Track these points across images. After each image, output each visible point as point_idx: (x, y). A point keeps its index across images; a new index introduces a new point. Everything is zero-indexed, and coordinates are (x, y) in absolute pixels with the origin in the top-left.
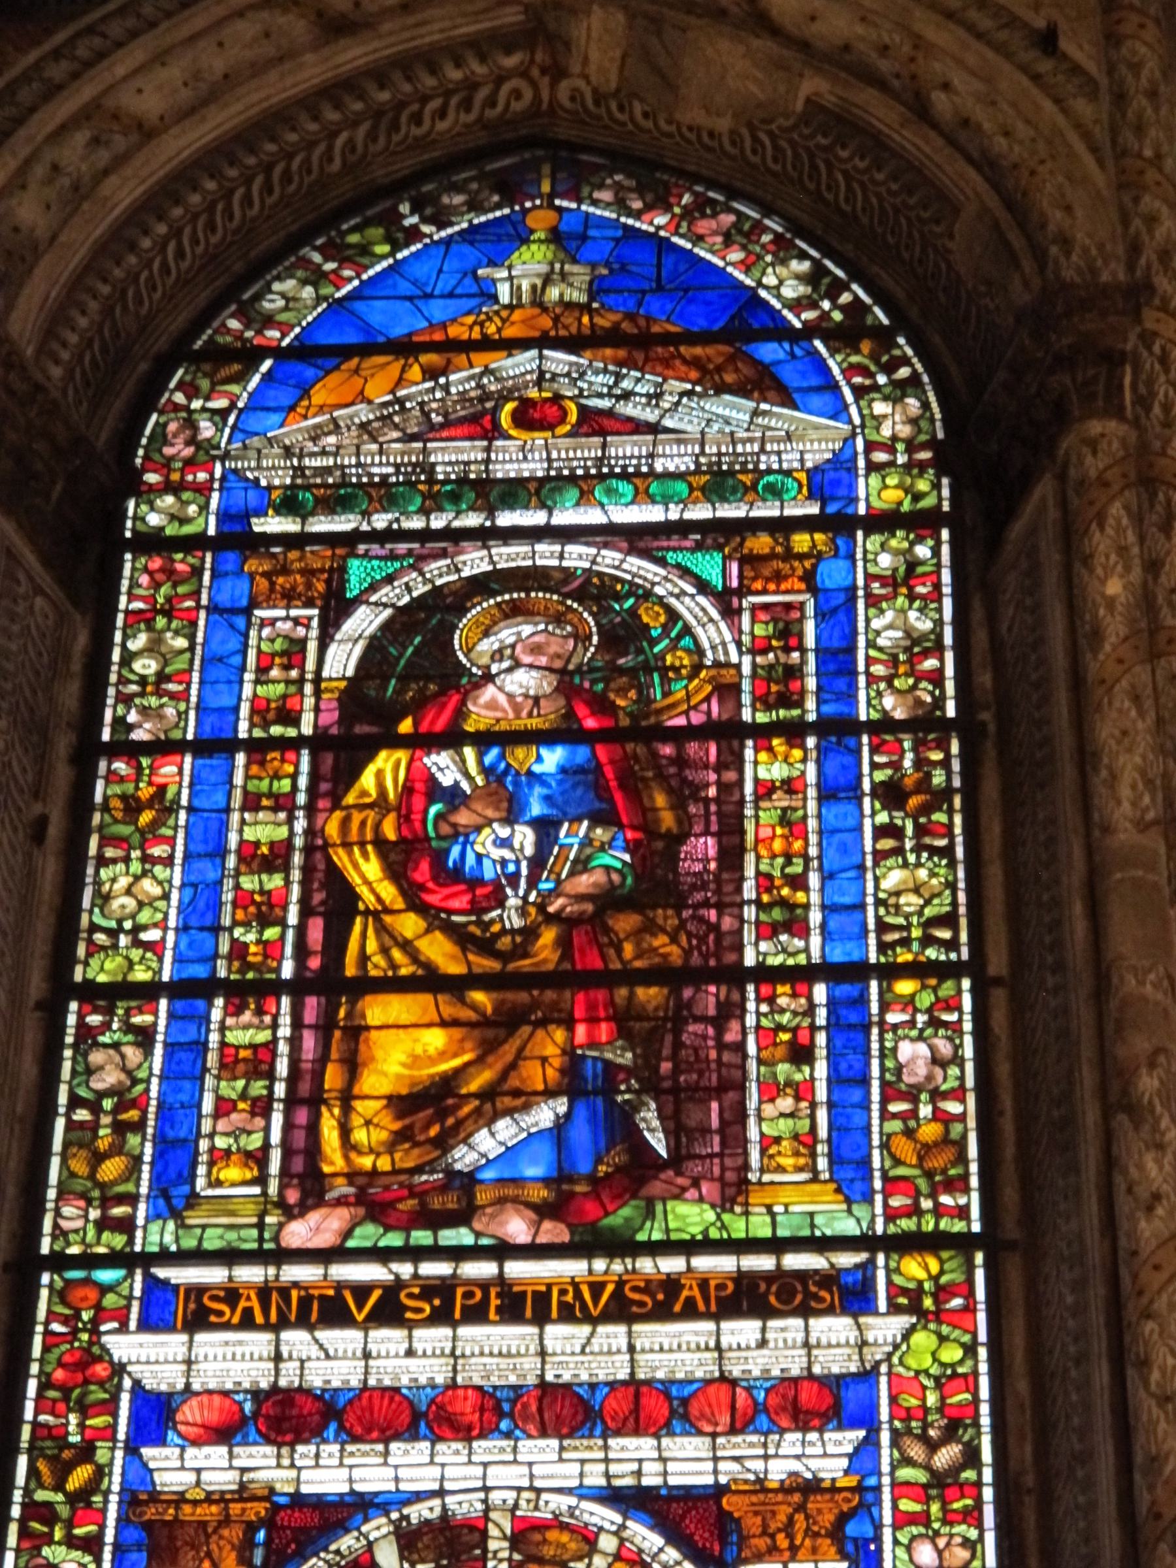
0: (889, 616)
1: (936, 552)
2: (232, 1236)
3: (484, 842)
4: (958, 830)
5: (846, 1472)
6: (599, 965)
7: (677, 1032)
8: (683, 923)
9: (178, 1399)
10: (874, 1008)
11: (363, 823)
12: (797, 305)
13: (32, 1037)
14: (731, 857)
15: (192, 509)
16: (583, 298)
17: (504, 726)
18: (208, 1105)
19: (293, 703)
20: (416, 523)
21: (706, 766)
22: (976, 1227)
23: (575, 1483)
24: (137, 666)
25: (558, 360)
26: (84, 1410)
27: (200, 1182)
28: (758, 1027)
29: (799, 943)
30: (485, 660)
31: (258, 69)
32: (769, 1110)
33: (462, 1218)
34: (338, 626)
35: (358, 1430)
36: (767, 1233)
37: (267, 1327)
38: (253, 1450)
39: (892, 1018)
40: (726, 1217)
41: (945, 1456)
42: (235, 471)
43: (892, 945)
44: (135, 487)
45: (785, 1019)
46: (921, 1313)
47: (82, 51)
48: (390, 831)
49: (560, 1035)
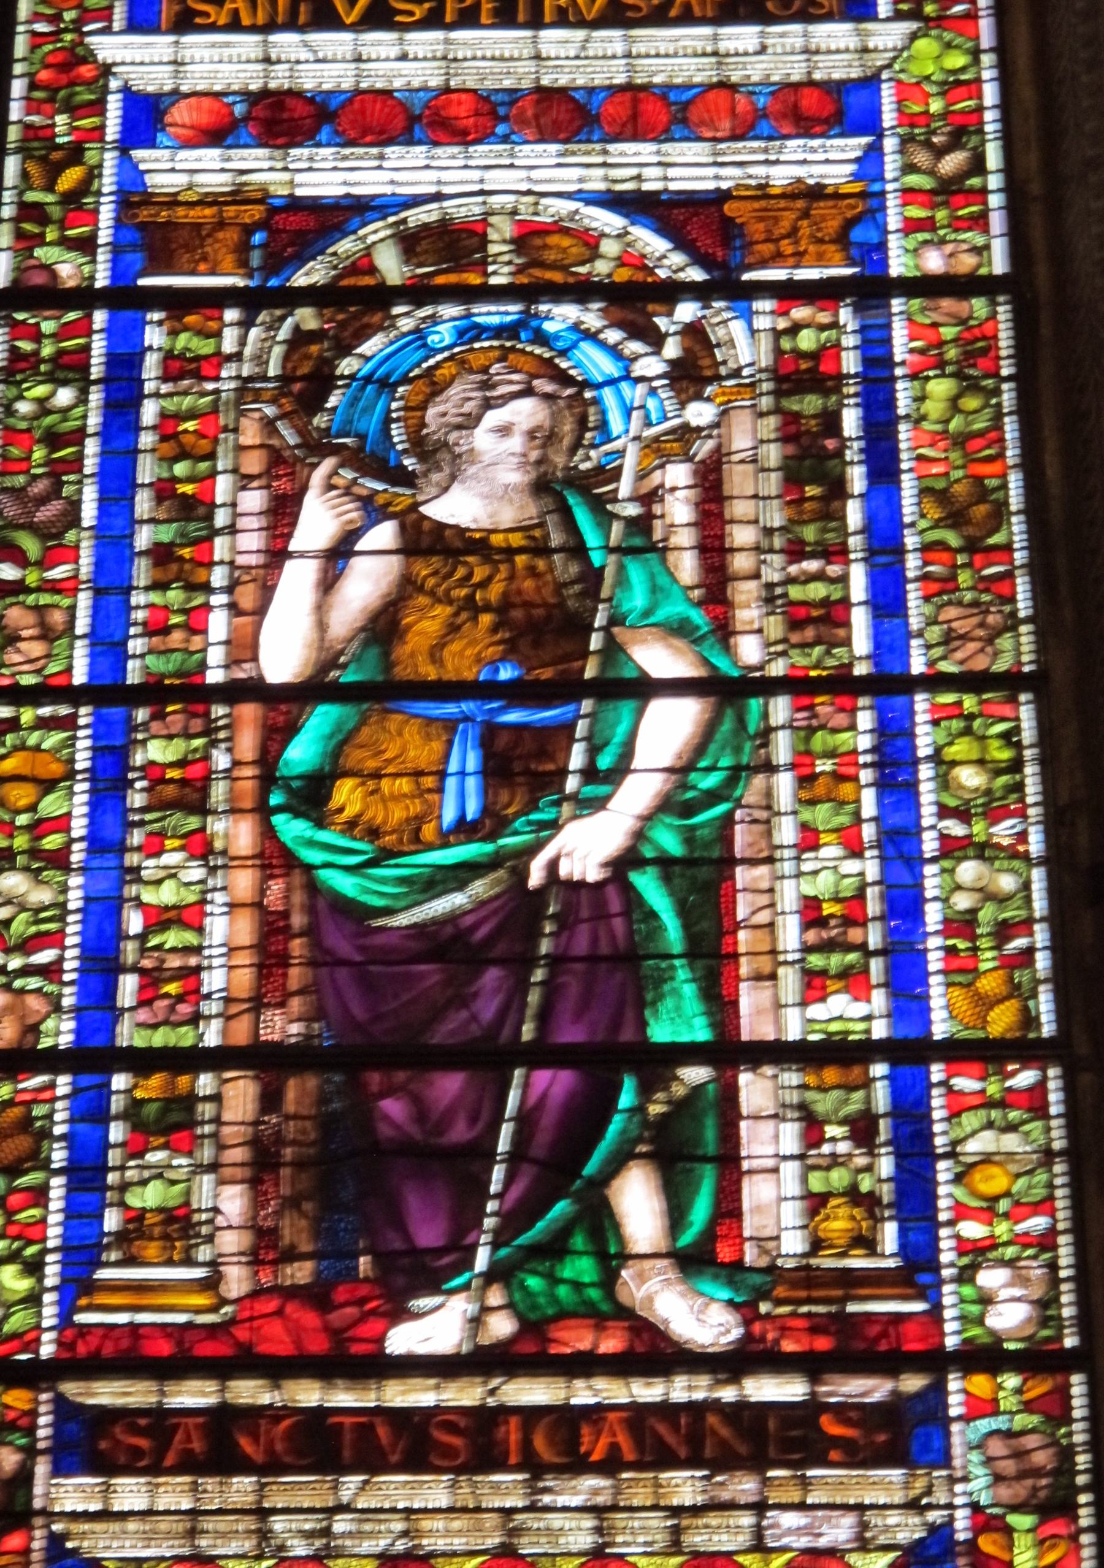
9: (167, 101)
37: (253, 29)
38: (245, 152)
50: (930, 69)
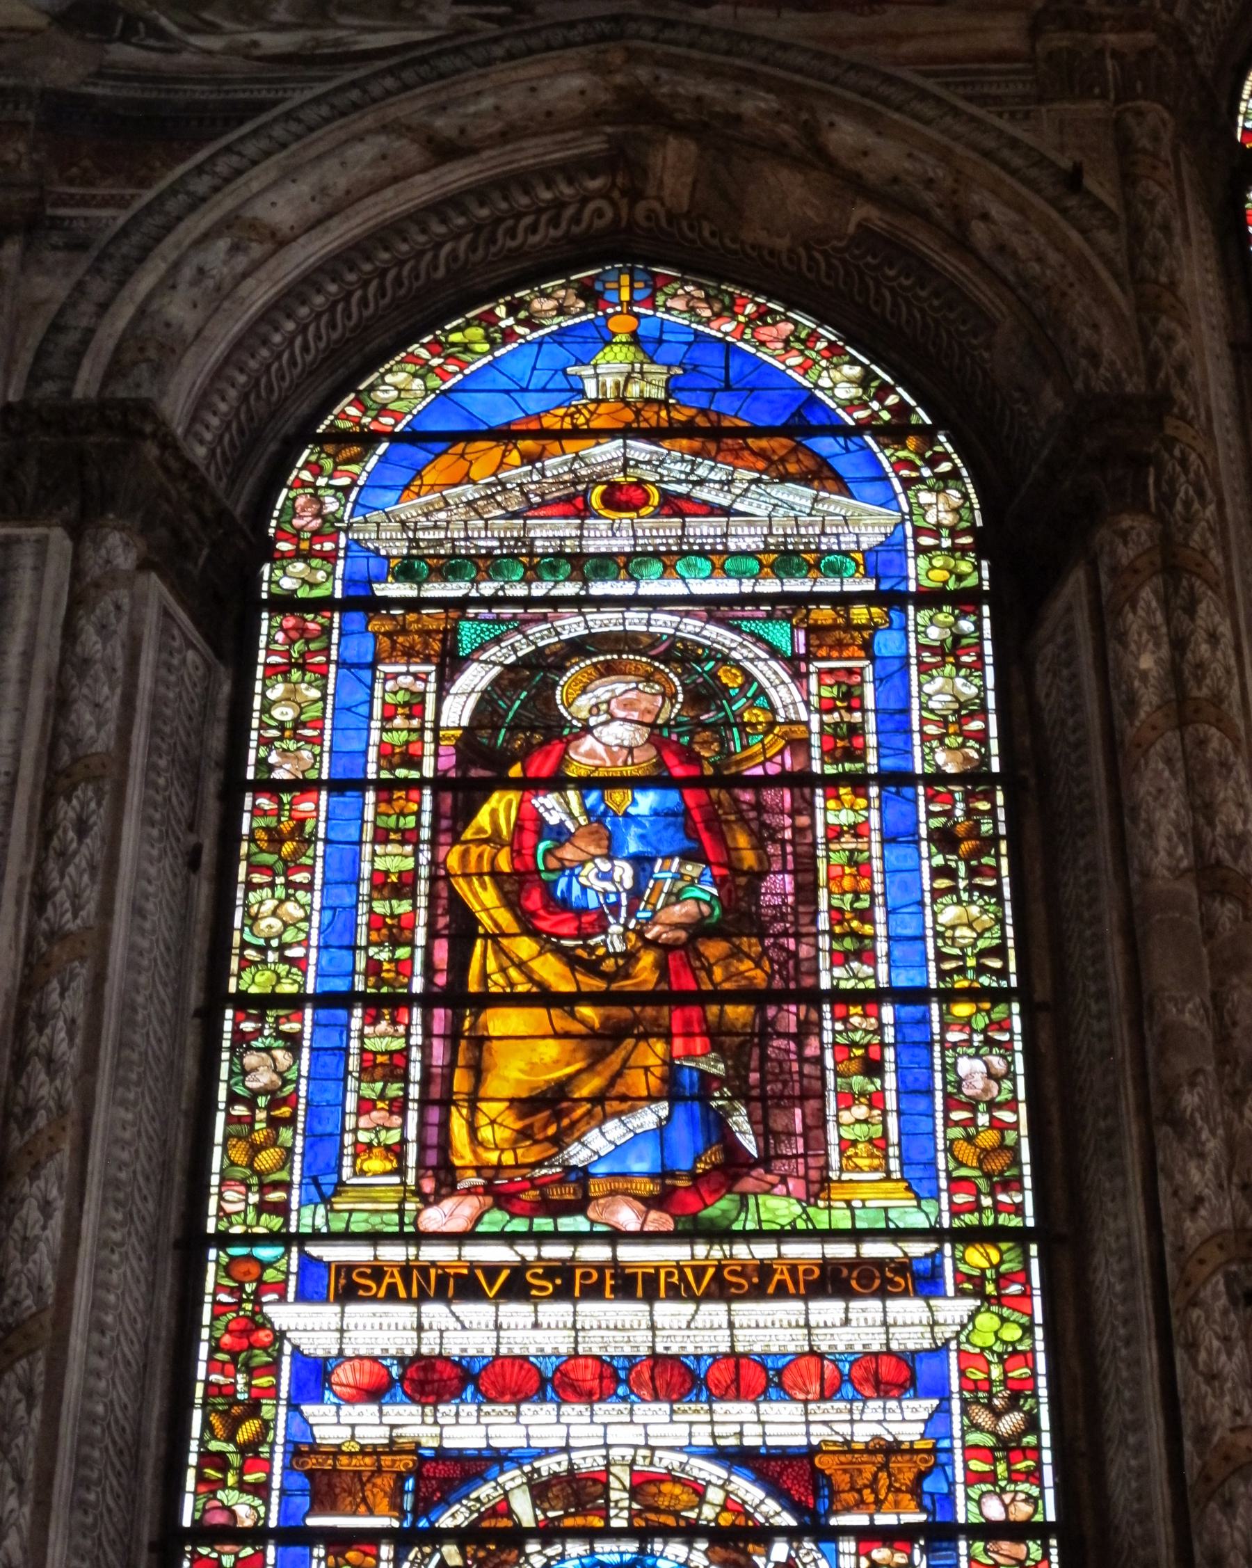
0: (939, 682)
1: (979, 626)
2: (376, 1219)
3: (588, 874)
4: (1005, 871)
5: (923, 1436)
6: (693, 987)
7: (763, 1047)
8: (765, 951)
9: (333, 1363)
10: (936, 1028)
11: (480, 856)
12: (850, 406)
13: (192, 1039)
14: (807, 892)
15: (321, 576)
16: (661, 395)
17: (601, 773)
18: (351, 1103)
19: (414, 749)
20: (519, 591)
21: (782, 812)
22: (1030, 1223)
23: (685, 1442)
24: (276, 713)
25: (640, 449)
26: (251, 1372)
27: (346, 1173)
28: (835, 1044)
29: (868, 970)
30: (584, 714)
31: (376, 188)
32: (846, 1117)
33: (579, 1207)
34: (453, 681)
35: (493, 1393)
36: (847, 1225)
37: (409, 1300)
38: (401, 1408)
39: (953, 1037)
40: (811, 1210)
41: (1010, 1423)
42: (357, 541)
43: (950, 973)
44: (270, 554)
45: (857, 1036)
46: (986, 1298)
47: (222, 167)
48: (504, 864)
49: (660, 1047)
50: (990, 1340)
